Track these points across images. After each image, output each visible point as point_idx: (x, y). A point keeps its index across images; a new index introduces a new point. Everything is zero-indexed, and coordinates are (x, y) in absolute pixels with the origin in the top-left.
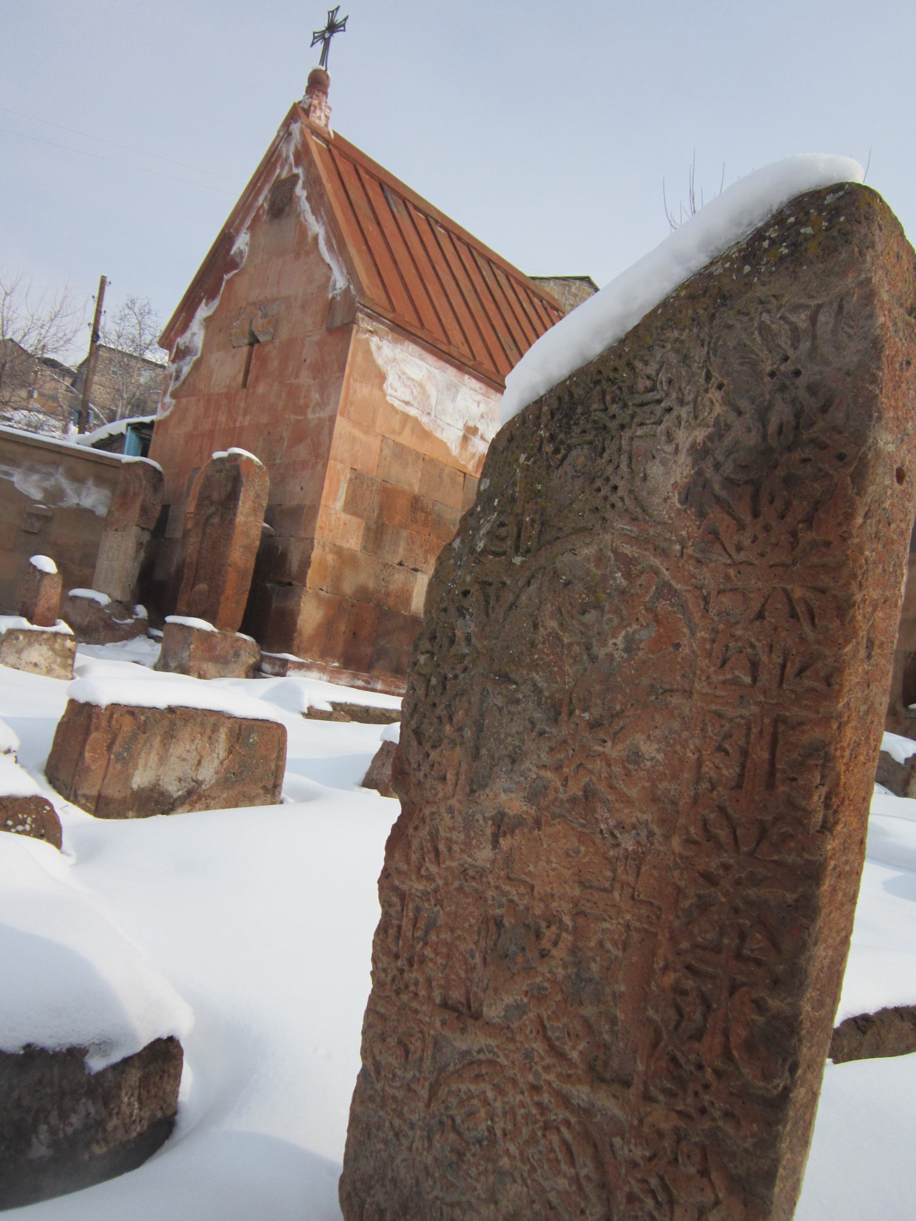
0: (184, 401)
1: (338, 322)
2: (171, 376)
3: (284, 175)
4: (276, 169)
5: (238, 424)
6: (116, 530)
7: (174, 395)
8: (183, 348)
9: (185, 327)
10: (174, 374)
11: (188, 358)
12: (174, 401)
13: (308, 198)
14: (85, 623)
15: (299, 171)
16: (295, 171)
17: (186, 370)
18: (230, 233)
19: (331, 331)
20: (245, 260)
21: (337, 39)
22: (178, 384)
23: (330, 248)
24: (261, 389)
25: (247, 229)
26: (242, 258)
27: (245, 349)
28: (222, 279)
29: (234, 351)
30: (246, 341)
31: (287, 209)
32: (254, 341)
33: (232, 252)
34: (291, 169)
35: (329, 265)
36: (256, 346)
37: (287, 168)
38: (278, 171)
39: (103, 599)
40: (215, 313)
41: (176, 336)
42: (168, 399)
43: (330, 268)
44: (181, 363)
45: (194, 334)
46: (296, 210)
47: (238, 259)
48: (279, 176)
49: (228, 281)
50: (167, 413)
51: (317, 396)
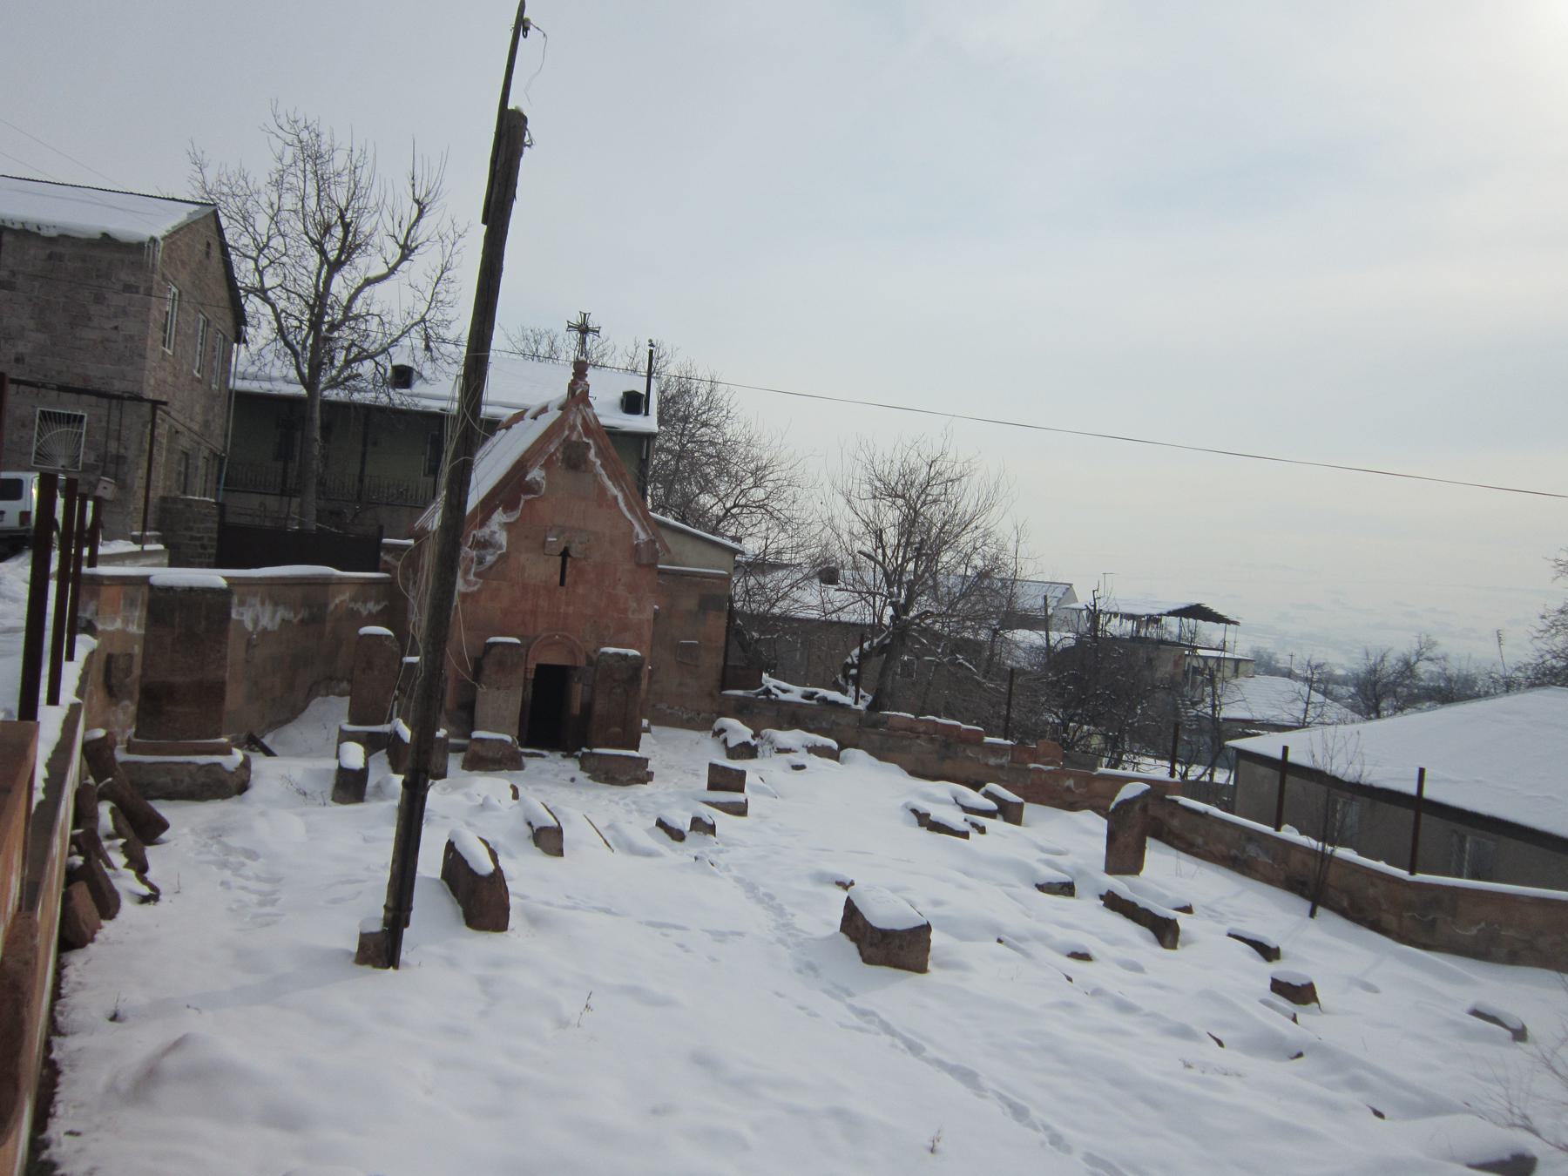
0: (495, 584)
1: (644, 561)
2: (472, 560)
3: (574, 437)
4: (564, 430)
5: (562, 611)
6: (498, 689)
7: (476, 575)
8: (482, 540)
9: (483, 524)
10: (475, 559)
11: (491, 550)
12: (481, 581)
13: (601, 465)
14: (499, 756)
15: (591, 442)
16: (587, 441)
17: (490, 559)
18: (526, 466)
19: (639, 565)
20: (543, 490)
21: (590, 337)
22: (482, 568)
23: (631, 509)
24: (580, 590)
25: (541, 466)
26: (540, 488)
27: (560, 558)
28: (520, 498)
29: (546, 557)
30: (559, 553)
31: (583, 466)
32: (565, 554)
33: (527, 479)
34: (580, 437)
35: (631, 521)
36: (569, 559)
37: (576, 433)
38: (567, 433)
39: (508, 738)
40: (517, 521)
41: (472, 529)
42: (471, 577)
43: (632, 524)
44: (483, 552)
45: (494, 533)
46: (592, 471)
47: (536, 487)
48: (567, 436)
49: (526, 501)
50: (475, 588)
51: (635, 605)
